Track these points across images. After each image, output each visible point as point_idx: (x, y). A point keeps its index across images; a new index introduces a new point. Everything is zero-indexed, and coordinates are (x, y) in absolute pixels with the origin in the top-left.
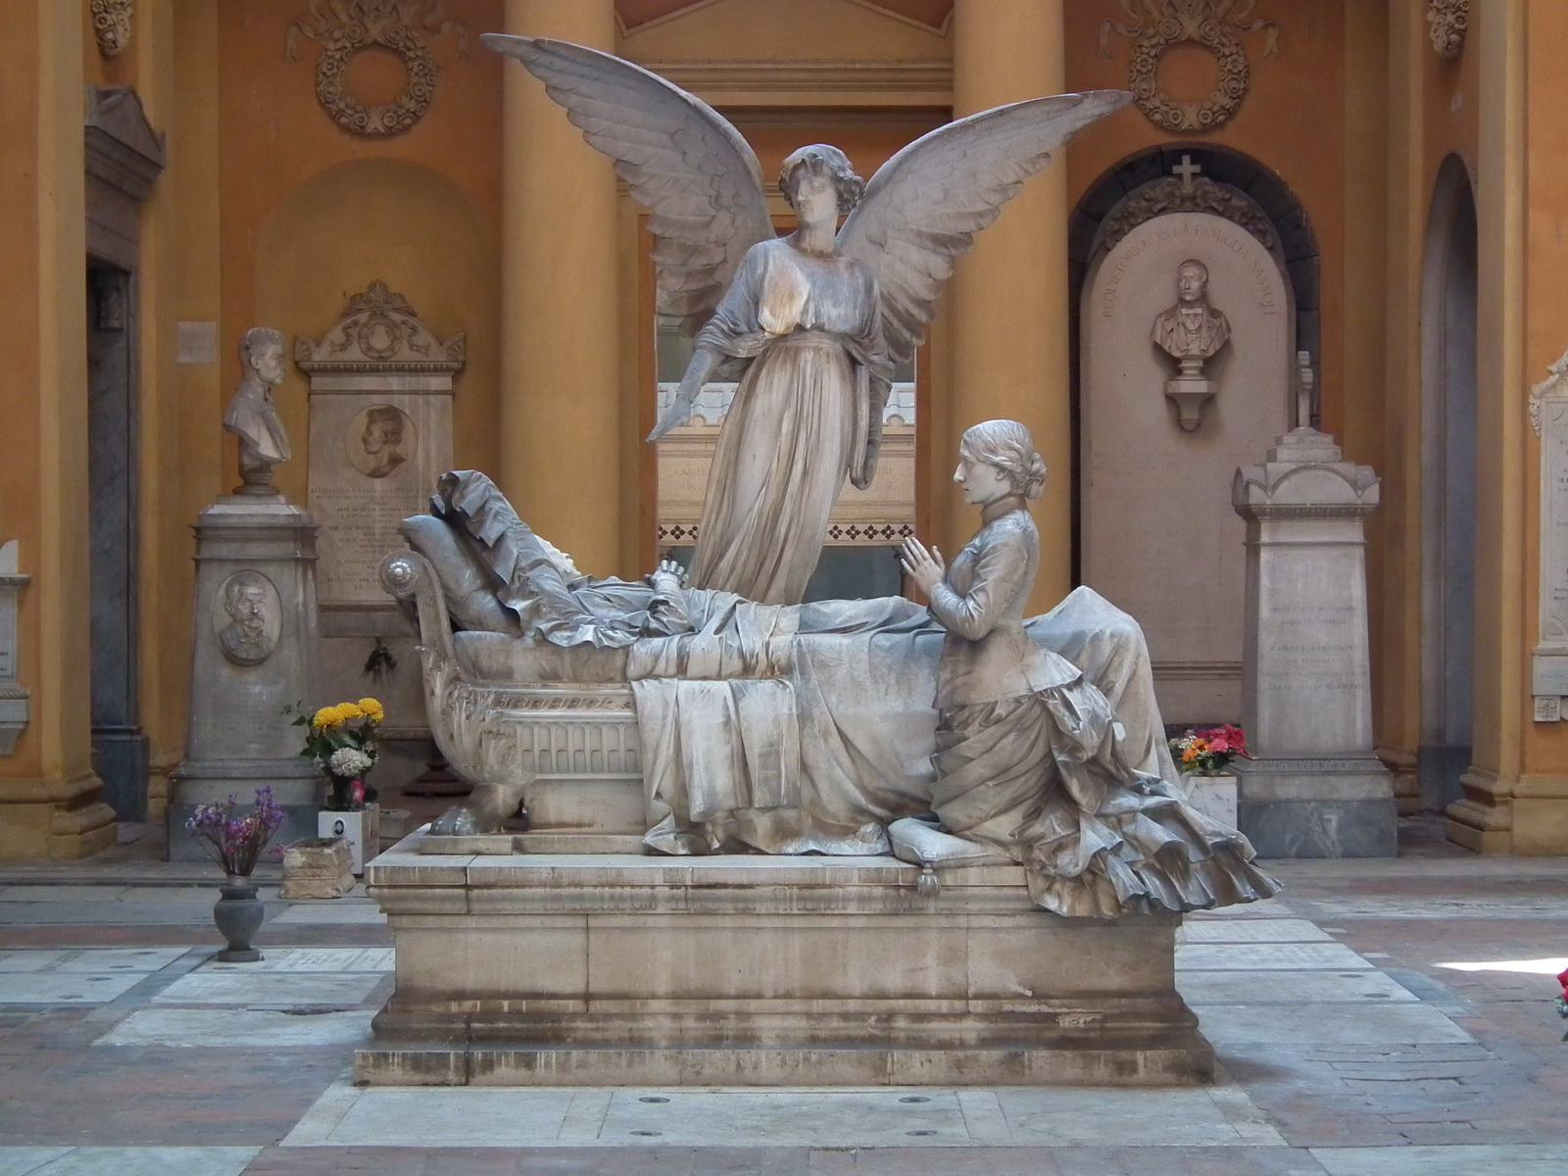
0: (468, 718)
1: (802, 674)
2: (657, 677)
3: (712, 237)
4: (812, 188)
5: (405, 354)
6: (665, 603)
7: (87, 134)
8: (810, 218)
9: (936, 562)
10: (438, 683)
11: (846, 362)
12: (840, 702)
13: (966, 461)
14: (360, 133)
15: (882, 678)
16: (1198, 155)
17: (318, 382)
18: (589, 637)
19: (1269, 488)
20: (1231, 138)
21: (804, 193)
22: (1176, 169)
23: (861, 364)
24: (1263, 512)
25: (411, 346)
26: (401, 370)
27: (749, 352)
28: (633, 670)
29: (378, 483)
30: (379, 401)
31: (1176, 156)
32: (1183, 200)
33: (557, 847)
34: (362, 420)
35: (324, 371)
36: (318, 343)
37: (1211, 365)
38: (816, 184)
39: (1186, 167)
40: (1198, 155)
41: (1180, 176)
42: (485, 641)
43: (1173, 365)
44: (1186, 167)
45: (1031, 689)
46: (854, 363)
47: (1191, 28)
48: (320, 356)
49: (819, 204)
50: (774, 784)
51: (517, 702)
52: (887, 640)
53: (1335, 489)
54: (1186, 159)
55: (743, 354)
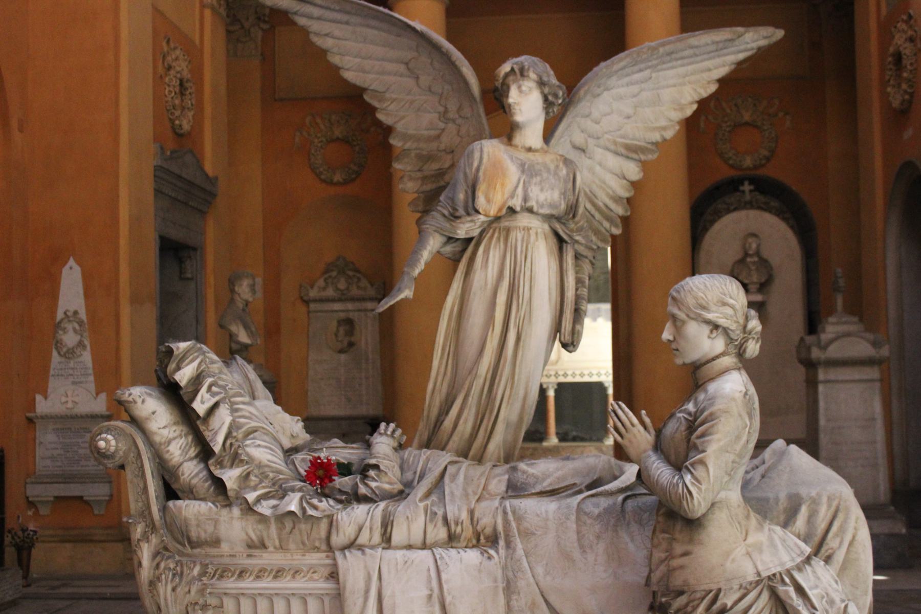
0: (174, 590)
1: (508, 544)
2: (361, 548)
3: (442, 147)
4: (521, 91)
5: (355, 291)
6: (376, 467)
7: (155, 170)
8: (519, 118)
9: (645, 428)
10: (145, 554)
11: (553, 241)
12: (547, 573)
13: (674, 318)
14: (331, 183)
15: (591, 547)
16: (753, 180)
17: (313, 306)
18: (293, 507)
19: (824, 348)
20: (769, 172)
21: (514, 96)
22: (741, 188)
23: (566, 242)
24: (819, 363)
25: (358, 287)
26: (353, 299)
27: (466, 233)
28: (338, 540)
29: (343, 357)
30: (342, 315)
31: (741, 181)
32: (746, 203)
34: (335, 323)
35: (315, 301)
36: (312, 287)
38: (524, 88)
39: (747, 187)
40: (753, 180)
41: (743, 192)
42: (193, 511)
44: (747, 187)
45: (759, 574)
46: (560, 241)
47: (747, 117)
48: (313, 293)
49: (527, 104)
51: (223, 573)
52: (597, 505)
53: (861, 348)
54: (746, 183)
55: (462, 233)
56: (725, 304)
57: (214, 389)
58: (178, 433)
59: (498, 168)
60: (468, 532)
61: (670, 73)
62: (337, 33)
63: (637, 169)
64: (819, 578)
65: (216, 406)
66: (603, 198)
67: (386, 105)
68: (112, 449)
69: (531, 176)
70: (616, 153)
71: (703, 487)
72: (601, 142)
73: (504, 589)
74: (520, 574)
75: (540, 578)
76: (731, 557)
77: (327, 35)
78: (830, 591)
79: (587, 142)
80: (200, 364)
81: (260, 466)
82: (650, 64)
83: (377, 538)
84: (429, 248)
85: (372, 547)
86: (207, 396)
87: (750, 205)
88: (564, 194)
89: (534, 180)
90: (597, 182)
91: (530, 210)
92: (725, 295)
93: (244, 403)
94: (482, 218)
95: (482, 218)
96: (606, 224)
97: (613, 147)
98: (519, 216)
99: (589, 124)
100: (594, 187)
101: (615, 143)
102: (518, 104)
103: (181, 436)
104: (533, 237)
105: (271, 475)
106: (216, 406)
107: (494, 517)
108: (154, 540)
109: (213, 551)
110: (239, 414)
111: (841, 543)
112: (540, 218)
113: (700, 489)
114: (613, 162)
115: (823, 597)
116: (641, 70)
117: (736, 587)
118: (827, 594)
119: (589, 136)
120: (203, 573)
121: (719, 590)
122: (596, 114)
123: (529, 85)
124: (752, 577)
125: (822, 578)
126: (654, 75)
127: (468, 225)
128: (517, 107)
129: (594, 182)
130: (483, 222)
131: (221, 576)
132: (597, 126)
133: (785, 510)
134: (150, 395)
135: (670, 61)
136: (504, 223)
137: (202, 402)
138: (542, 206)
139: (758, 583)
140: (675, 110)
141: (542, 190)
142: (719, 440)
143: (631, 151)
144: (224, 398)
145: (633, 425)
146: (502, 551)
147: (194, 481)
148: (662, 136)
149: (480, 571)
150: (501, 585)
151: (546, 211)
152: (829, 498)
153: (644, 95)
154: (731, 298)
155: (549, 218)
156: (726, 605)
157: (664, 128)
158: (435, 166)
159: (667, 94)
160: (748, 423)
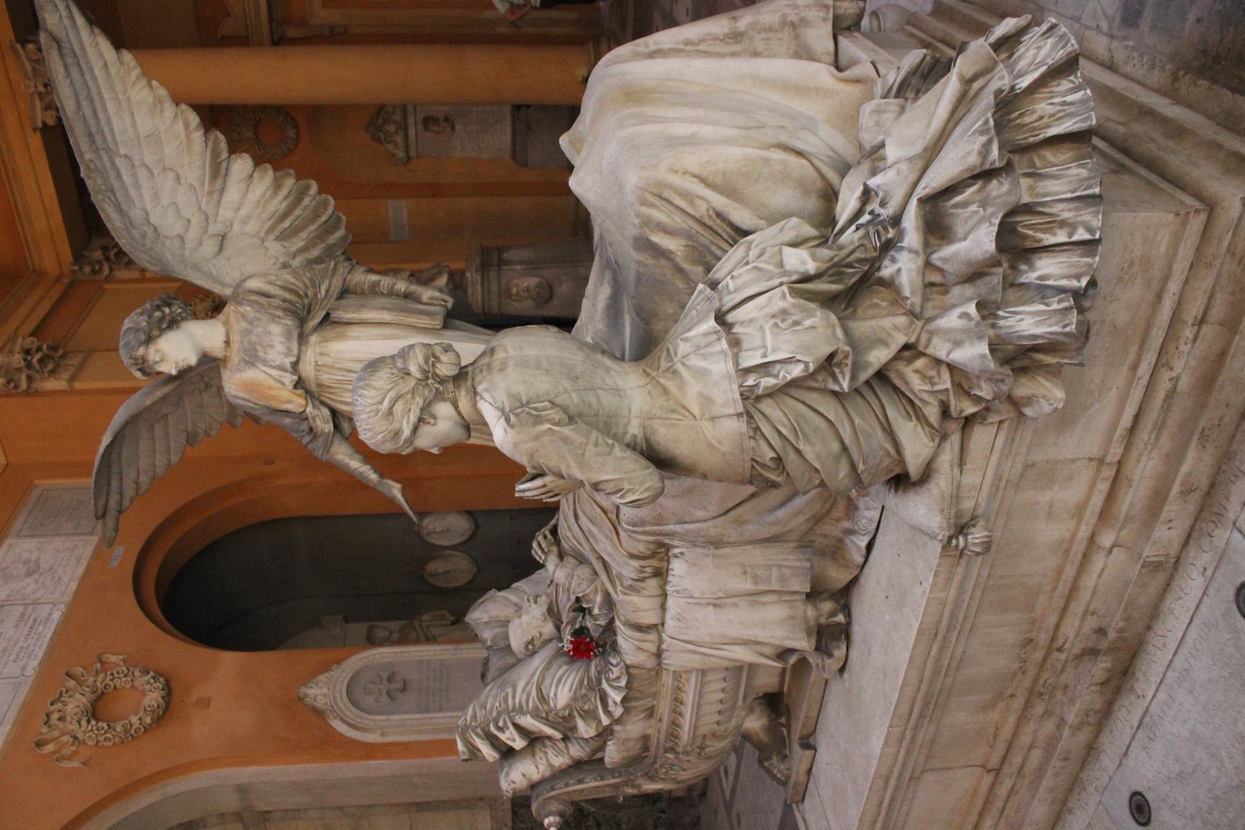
0: (684, 770)
4: (162, 360)
10: (650, 787)
11: (330, 332)
12: (704, 508)
14: (298, 139)
17: (412, 154)
21: (170, 368)
25: (394, 113)
26: (405, 117)
29: (458, 127)
30: (420, 127)
33: (814, 713)
34: (429, 135)
35: (407, 152)
36: (395, 155)
38: (157, 359)
45: (739, 415)
48: (401, 154)
50: (788, 572)
51: (673, 736)
55: (328, 427)
56: (390, 412)
57: (501, 724)
58: (542, 755)
59: (251, 387)
60: (654, 563)
61: (116, 124)
62: (133, 475)
63: (239, 161)
64: (751, 321)
65: (517, 727)
66: (279, 203)
68: (557, 819)
69: (257, 357)
70: (223, 189)
71: (627, 487)
72: (211, 212)
73: (716, 548)
74: (702, 533)
75: (709, 515)
76: (716, 444)
77: (137, 484)
78: (768, 310)
79: (212, 236)
80: (477, 735)
81: (575, 699)
82: (108, 165)
83: (653, 636)
84: (347, 460)
85: (661, 641)
86: (507, 733)
88: (274, 318)
89: (261, 354)
90: (258, 211)
91: (295, 365)
92: (378, 411)
93: (514, 697)
94: (309, 409)
95: (309, 409)
96: (307, 201)
97: (216, 196)
98: (304, 375)
99: (191, 236)
100: (265, 215)
101: (211, 193)
102: (177, 363)
103: (545, 753)
104: (327, 360)
105: (584, 691)
106: (517, 727)
107: (639, 541)
108: (640, 781)
109: (653, 742)
110: (524, 705)
111: (702, 198)
112: (304, 348)
113: (628, 491)
114: (233, 193)
115: (776, 325)
116: (119, 175)
117: (752, 443)
118: (773, 316)
119: (206, 232)
120: (673, 750)
121: (753, 460)
122: (178, 228)
123: (152, 353)
124: (741, 426)
125: (752, 315)
126: (122, 152)
127: (318, 423)
128: (181, 364)
129: (259, 215)
130: (314, 407)
131: (677, 737)
132: (193, 224)
133: (653, 257)
134: (507, 774)
135: (102, 133)
136: (313, 388)
137: (514, 740)
138: (290, 350)
139: (750, 416)
140: (162, 111)
141: (272, 347)
142: (568, 466)
143: (218, 172)
144: (510, 718)
145: (544, 486)
146: (676, 543)
147: (587, 749)
148: (196, 129)
149: (695, 565)
150: (713, 551)
151: (295, 345)
152: (644, 203)
153: (149, 159)
154: (381, 403)
155: (302, 338)
156: (772, 459)
157: (187, 126)
159: (145, 125)
160: (547, 426)
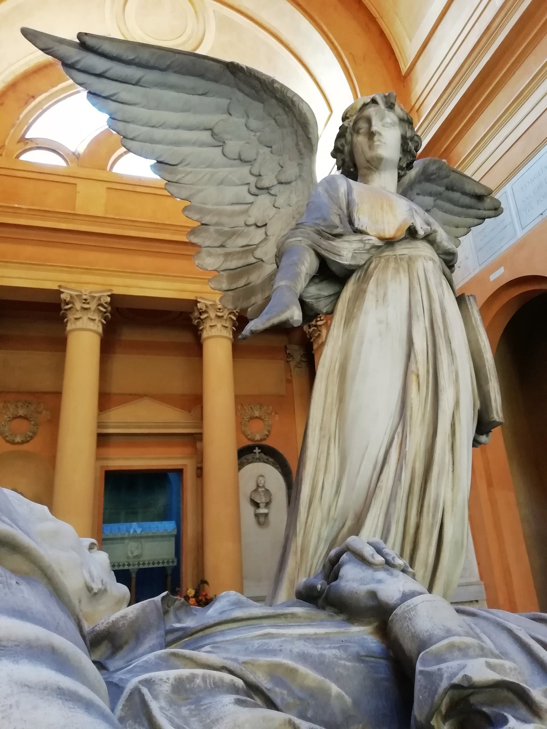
3: (251, 221)
14: (13, 443)
16: (260, 447)
20: (268, 442)
22: (254, 451)
27: (353, 257)
32: (257, 459)
37: (267, 504)
39: (257, 450)
40: (260, 447)
41: (255, 453)
43: (256, 505)
44: (257, 450)
47: (257, 414)
54: (257, 448)
67: (179, 176)
87: (259, 460)
158: (242, 241)
